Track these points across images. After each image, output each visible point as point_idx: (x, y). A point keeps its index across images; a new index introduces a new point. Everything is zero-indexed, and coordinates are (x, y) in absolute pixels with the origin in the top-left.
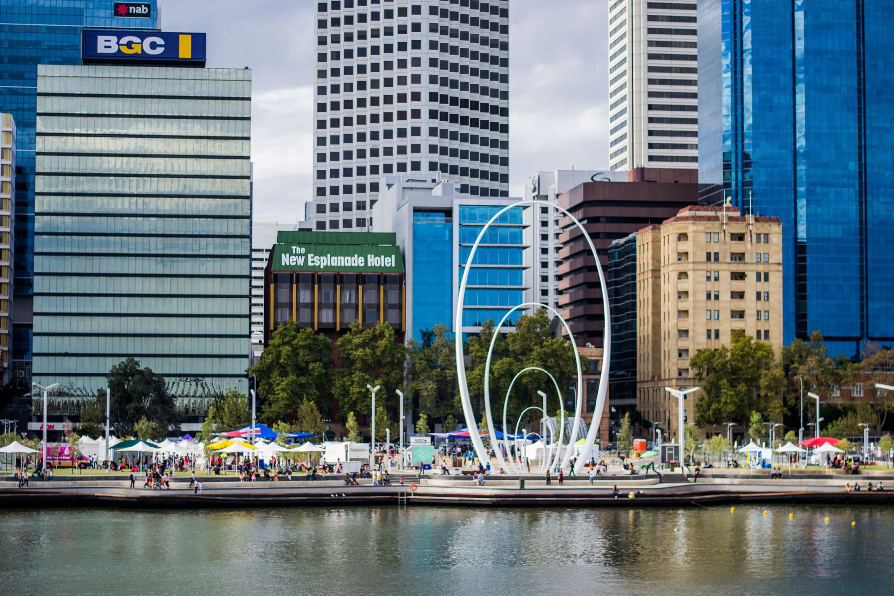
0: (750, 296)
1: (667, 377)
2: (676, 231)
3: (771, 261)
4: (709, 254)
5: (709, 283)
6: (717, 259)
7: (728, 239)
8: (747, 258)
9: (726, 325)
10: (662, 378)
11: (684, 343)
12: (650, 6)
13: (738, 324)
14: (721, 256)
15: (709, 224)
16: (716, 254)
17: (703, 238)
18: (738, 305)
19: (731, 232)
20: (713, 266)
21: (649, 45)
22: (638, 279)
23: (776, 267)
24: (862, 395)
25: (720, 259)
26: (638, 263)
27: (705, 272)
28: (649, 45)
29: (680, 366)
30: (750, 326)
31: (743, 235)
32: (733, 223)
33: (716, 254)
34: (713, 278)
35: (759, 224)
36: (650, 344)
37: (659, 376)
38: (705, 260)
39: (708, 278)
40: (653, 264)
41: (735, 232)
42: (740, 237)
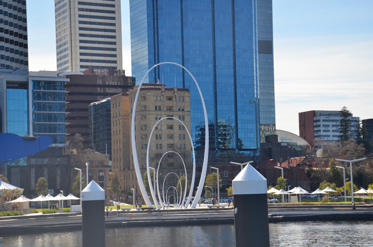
0: (176, 128)
3: (185, 110)
4: (156, 107)
6: (160, 109)
7: (165, 100)
8: (174, 109)
9: (165, 142)
13: (171, 142)
14: (162, 107)
15: (156, 92)
16: (160, 106)
17: (153, 99)
18: (171, 132)
19: (166, 96)
20: (159, 113)
21: (79, 10)
22: (112, 120)
23: (187, 113)
24: (227, 176)
25: (162, 110)
26: (111, 113)
28: (79, 10)
30: (176, 141)
31: (172, 97)
32: (167, 92)
35: (179, 92)
38: (154, 110)
41: (168, 96)
42: (170, 99)
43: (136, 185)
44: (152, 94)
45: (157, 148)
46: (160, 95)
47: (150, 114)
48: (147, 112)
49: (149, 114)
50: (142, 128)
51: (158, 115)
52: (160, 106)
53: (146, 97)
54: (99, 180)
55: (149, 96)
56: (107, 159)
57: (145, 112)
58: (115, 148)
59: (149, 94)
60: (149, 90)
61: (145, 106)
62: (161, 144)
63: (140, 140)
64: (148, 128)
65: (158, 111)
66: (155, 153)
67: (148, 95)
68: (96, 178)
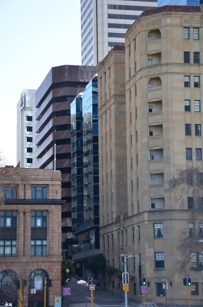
1: (135, 212)
2: (145, 28)
4: (187, 55)
5: (187, 90)
10: (130, 214)
11: (156, 167)
12: (111, 7)
16: (197, 54)
17: (179, 34)
20: (193, 69)
21: (108, 8)
27: (182, 76)
28: (108, 8)
29: (152, 195)
33: (197, 54)
34: (192, 85)
36: (114, 180)
37: (126, 214)
38: (182, 61)
39: (187, 84)
40: (115, 88)
43: (140, 255)
44: (177, 21)
45: (189, 158)
46: (198, 25)
47: (170, 71)
48: (164, 69)
49: (167, 73)
50: (150, 110)
51: (192, 77)
52: (198, 53)
53: (162, 31)
54: (32, 239)
55: (168, 28)
56: (54, 183)
57: (159, 68)
58: (104, 173)
59: (169, 21)
60: (169, 12)
61: (158, 55)
62: (201, 149)
63: (145, 140)
64: (164, 109)
65: (190, 65)
66: (184, 168)
67: (167, 26)
68: (24, 233)
